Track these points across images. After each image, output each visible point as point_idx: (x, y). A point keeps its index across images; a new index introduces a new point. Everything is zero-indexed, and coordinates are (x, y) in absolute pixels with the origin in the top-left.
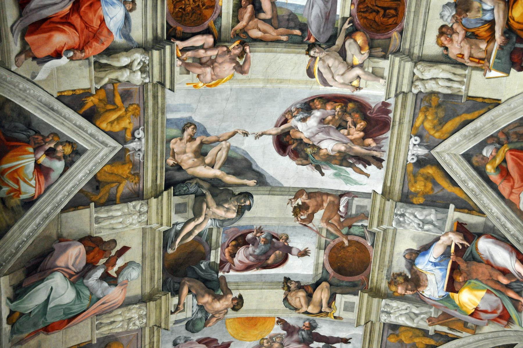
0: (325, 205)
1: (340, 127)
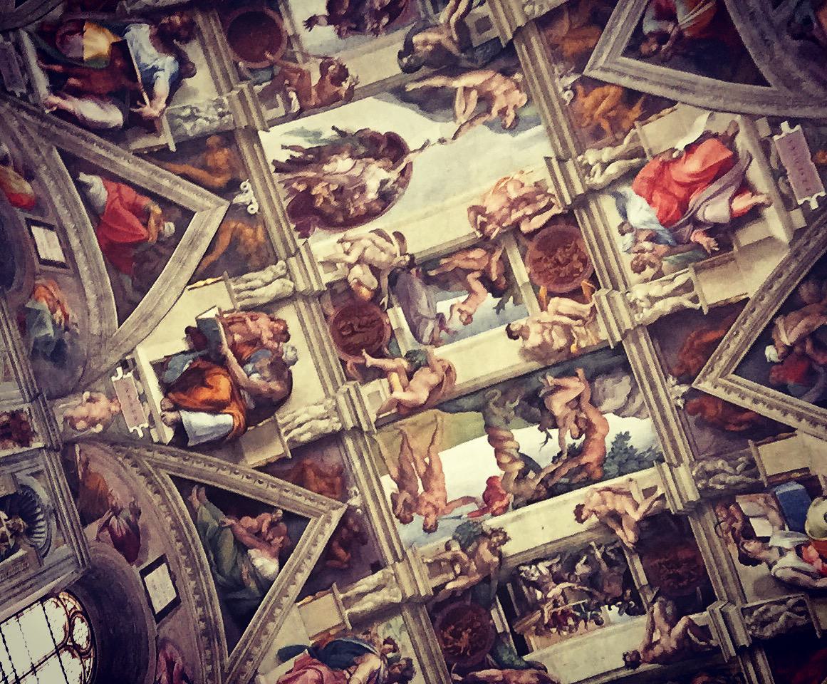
0: (314, 92)
1: (340, 192)
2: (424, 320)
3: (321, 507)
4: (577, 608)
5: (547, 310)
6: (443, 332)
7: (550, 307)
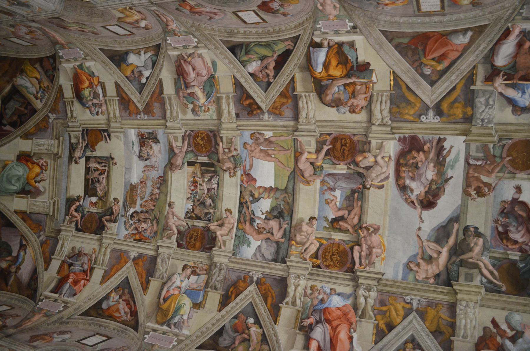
0: (476, 175)
1: (417, 167)
3: (268, 100)
4: (196, 193)
5: (315, 239)
6: (326, 188)
7: (316, 241)
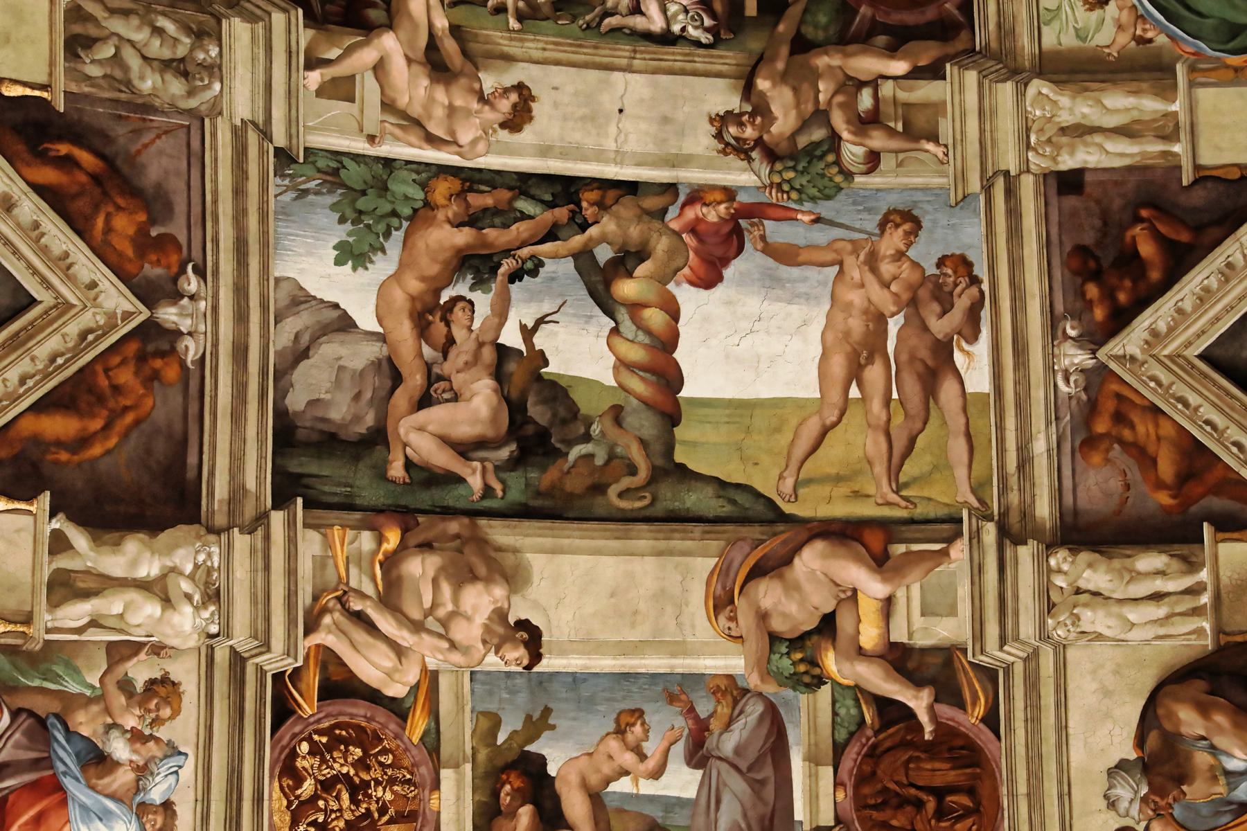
2: (744, 766)
3: (1164, 377)
5: (424, 669)
6: (703, 709)
7: (413, 676)
